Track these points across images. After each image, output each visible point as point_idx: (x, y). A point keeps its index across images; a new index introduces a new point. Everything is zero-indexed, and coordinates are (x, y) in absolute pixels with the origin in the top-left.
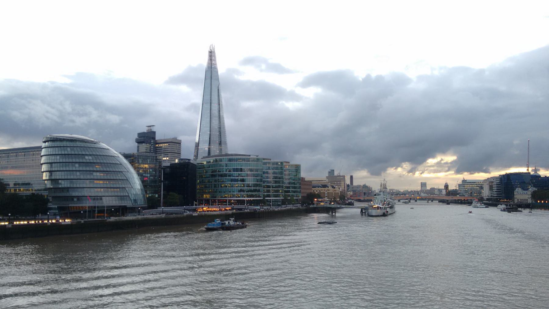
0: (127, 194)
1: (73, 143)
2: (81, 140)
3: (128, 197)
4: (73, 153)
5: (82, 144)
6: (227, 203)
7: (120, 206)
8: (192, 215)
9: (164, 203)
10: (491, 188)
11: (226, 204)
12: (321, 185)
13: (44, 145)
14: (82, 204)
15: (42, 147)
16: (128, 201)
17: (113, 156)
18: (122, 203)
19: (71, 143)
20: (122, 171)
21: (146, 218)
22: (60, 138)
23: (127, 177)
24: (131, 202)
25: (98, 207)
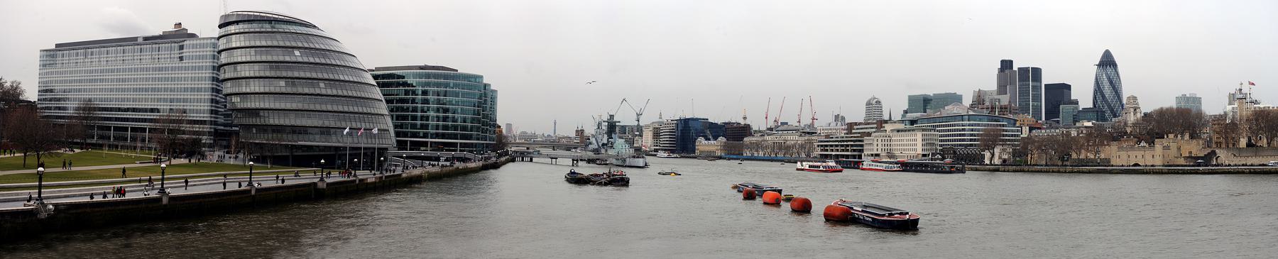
6: (427, 146)
10: (657, 134)
11: (424, 148)
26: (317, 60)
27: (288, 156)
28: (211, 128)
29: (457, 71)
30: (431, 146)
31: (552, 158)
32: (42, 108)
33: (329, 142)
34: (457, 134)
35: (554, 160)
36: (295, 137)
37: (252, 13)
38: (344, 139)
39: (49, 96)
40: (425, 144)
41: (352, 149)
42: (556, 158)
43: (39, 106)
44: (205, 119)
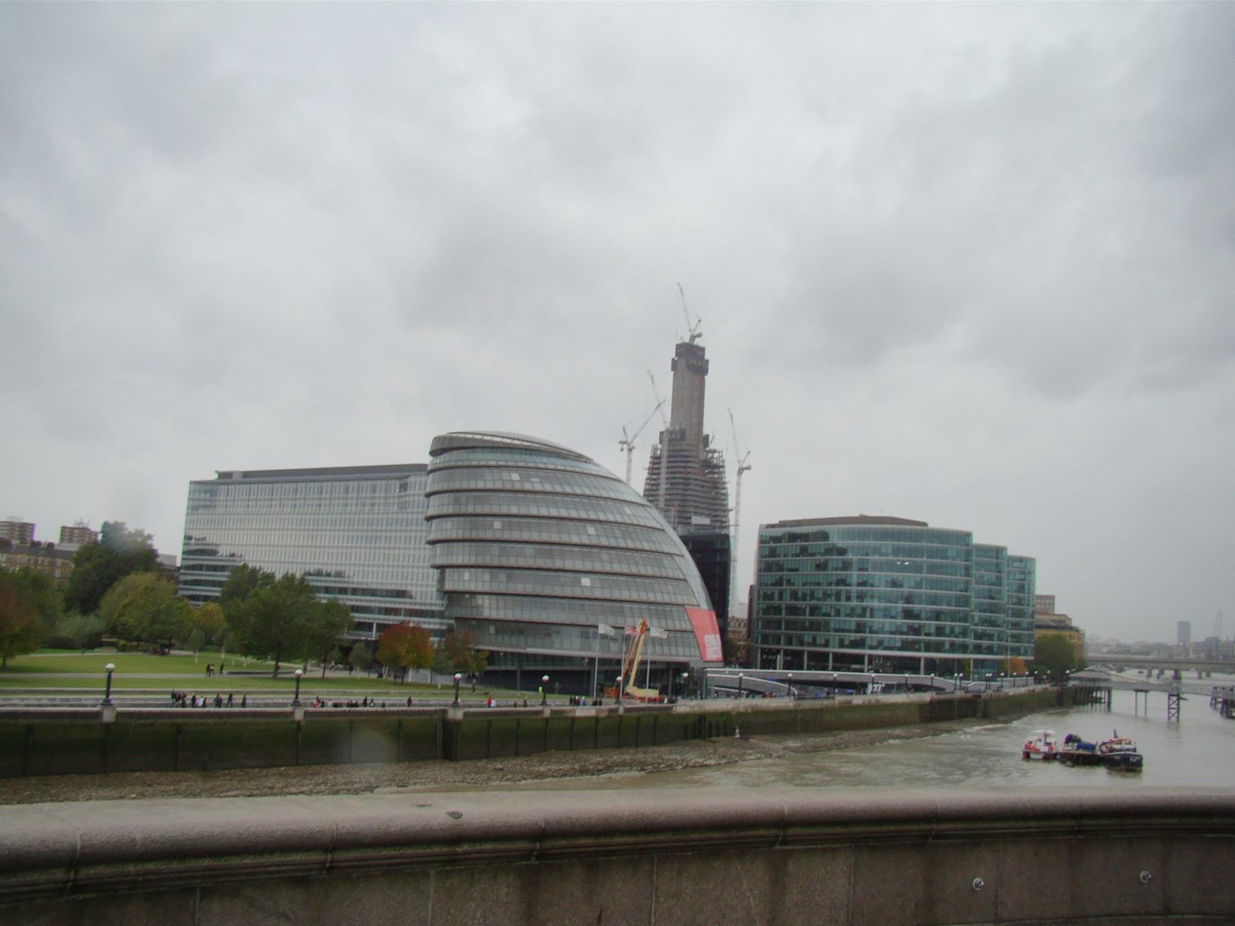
0: (689, 628)
1: (524, 457)
2: (552, 449)
3: (691, 636)
4: (528, 486)
5: (559, 464)
6: (863, 663)
7: (669, 664)
8: (850, 702)
9: (808, 665)
11: (858, 666)
12: (1052, 621)
13: (427, 459)
14: (551, 648)
15: (429, 468)
16: (692, 649)
17: (643, 505)
18: (677, 655)
19: (528, 458)
20: (671, 551)
21: (756, 705)
22: (493, 442)
23: (685, 572)
24: (698, 654)
25: (653, 663)
26: (564, 513)
27: (514, 672)
28: (442, 624)
29: (925, 524)
30: (870, 663)
31: (1137, 691)
32: (185, 583)
33: (546, 648)
34: (918, 642)
35: (1141, 695)
36: (522, 640)
37: (471, 436)
38: (568, 647)
39: (205, 560)
40: (859, 659)
41: (603, 661)
42: (1146, 691)
43: (182, 578)
44: (433, 608)
